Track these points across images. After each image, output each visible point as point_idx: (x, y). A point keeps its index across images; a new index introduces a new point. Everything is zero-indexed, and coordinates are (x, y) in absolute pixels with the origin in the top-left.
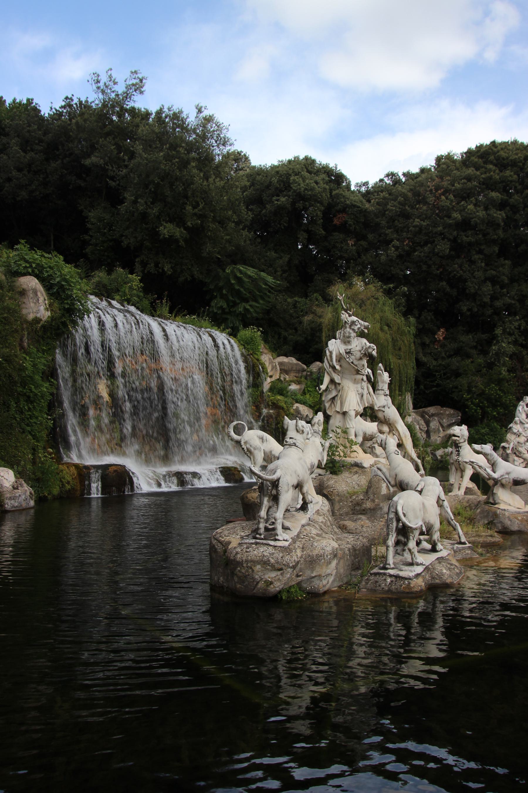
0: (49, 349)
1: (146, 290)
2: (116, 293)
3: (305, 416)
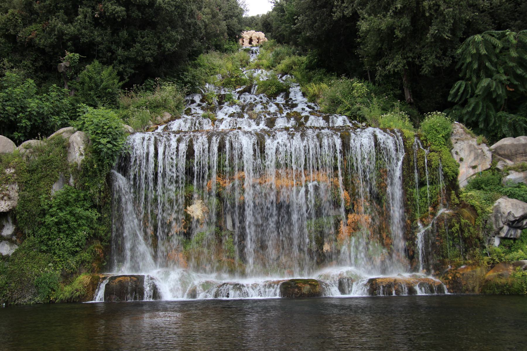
3: (506, 214)
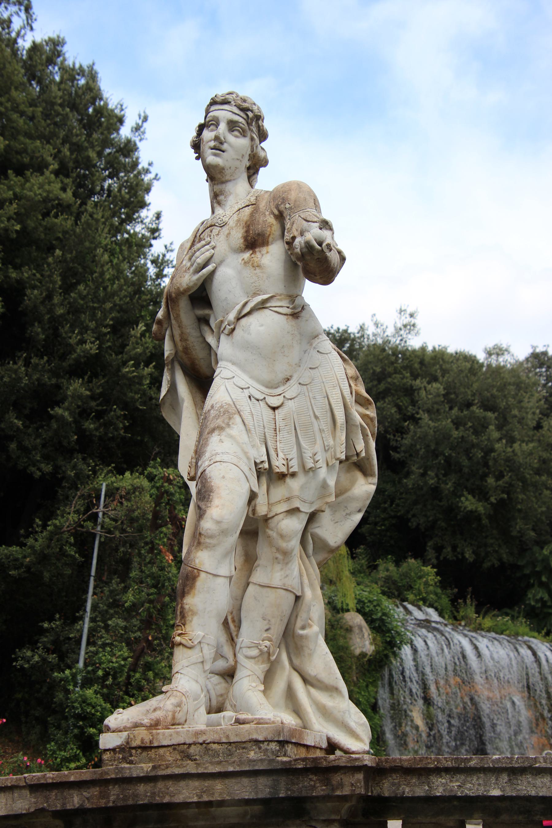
0: (374, 681)
1: (443, 585)
2: (409, 590)
